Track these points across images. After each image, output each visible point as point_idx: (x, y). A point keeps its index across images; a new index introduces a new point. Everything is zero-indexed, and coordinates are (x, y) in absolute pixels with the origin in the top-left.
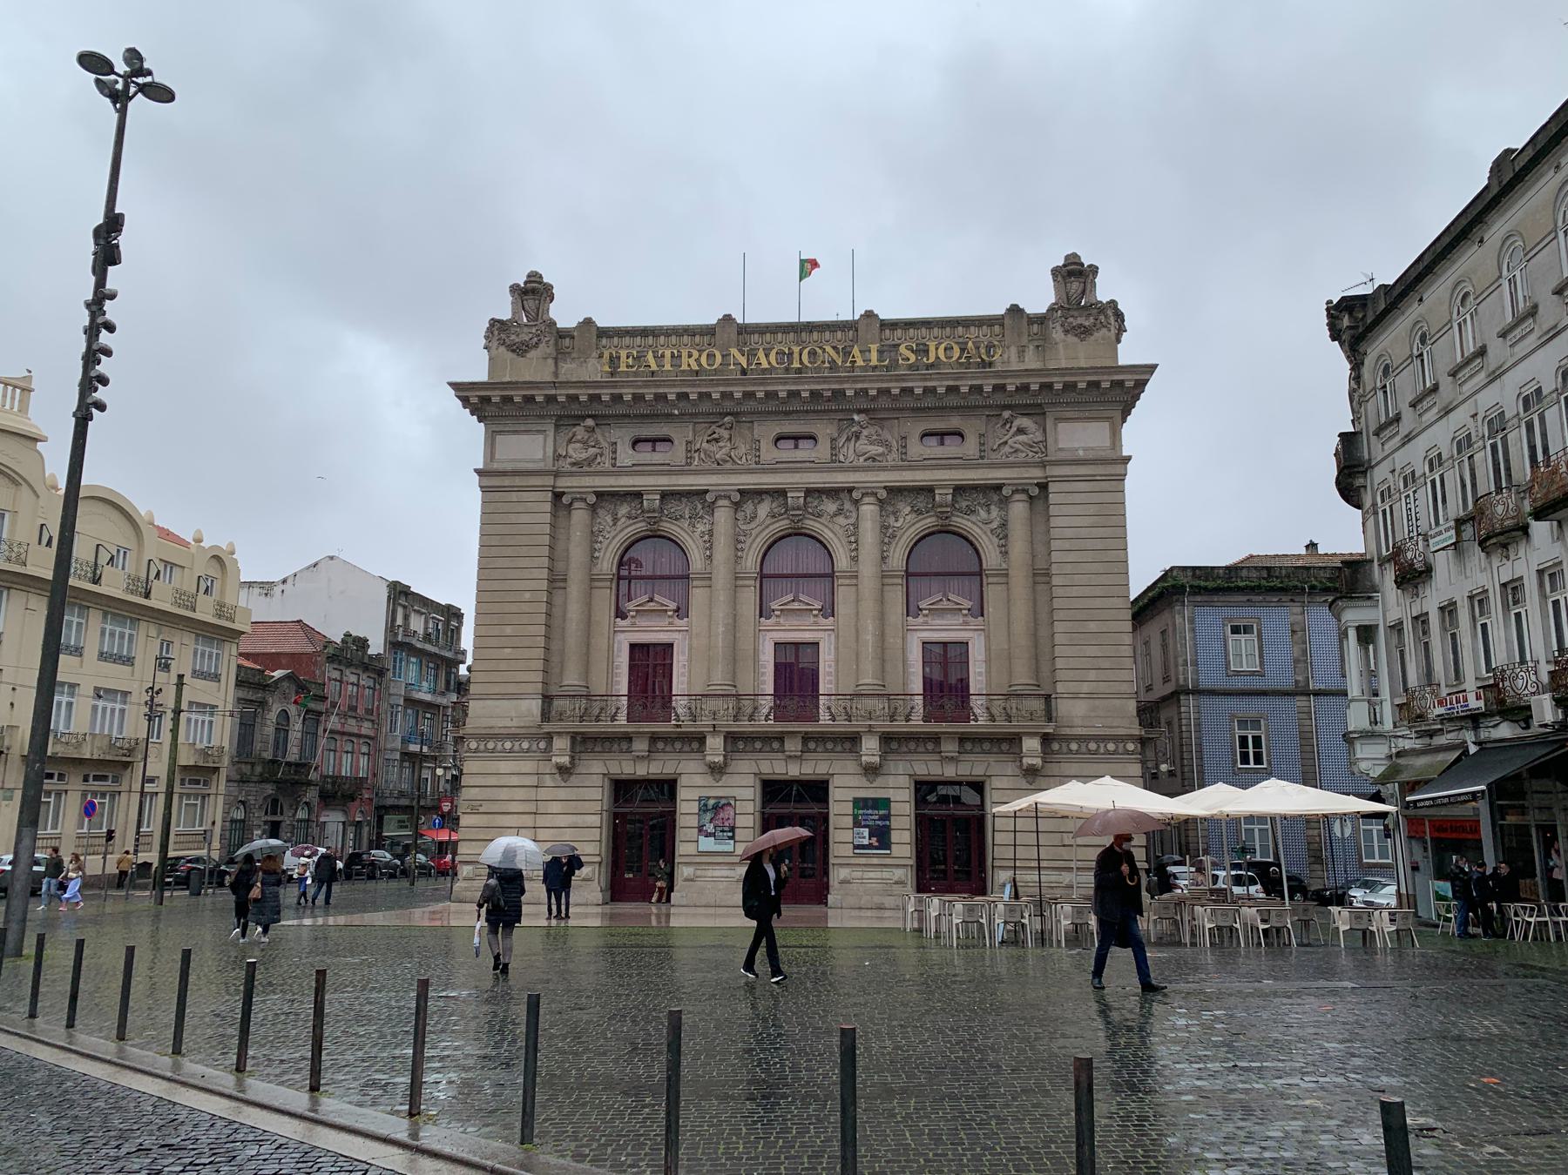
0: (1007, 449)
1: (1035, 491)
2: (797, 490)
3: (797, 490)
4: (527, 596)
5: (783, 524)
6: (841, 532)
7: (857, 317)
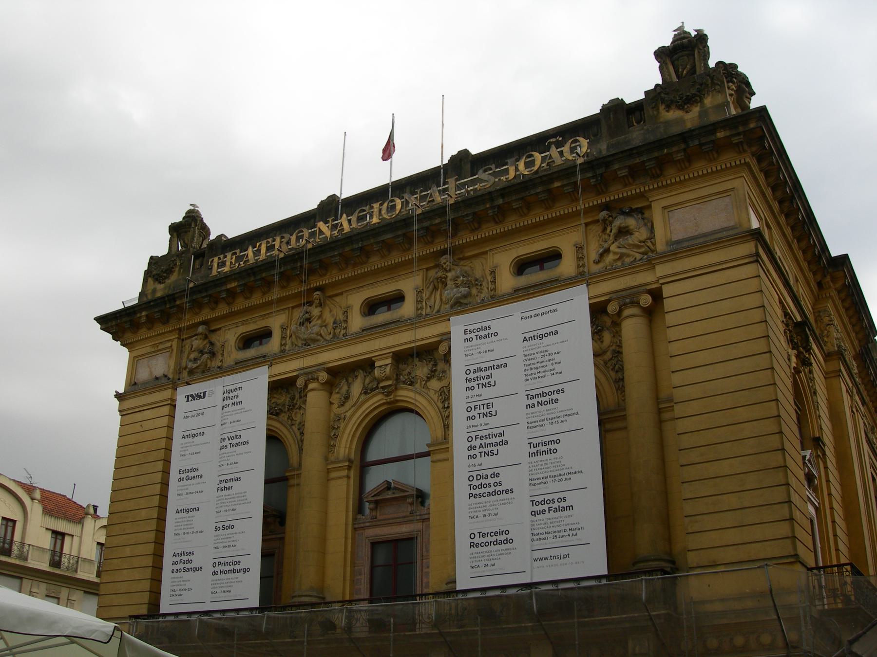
0: (610, 258)
1: (646, 300)
2: (382, 357)
3: (382, 357)
4: (143, 514)
5: (377, 399)
6: (435, 397)
7: (446, 161)
